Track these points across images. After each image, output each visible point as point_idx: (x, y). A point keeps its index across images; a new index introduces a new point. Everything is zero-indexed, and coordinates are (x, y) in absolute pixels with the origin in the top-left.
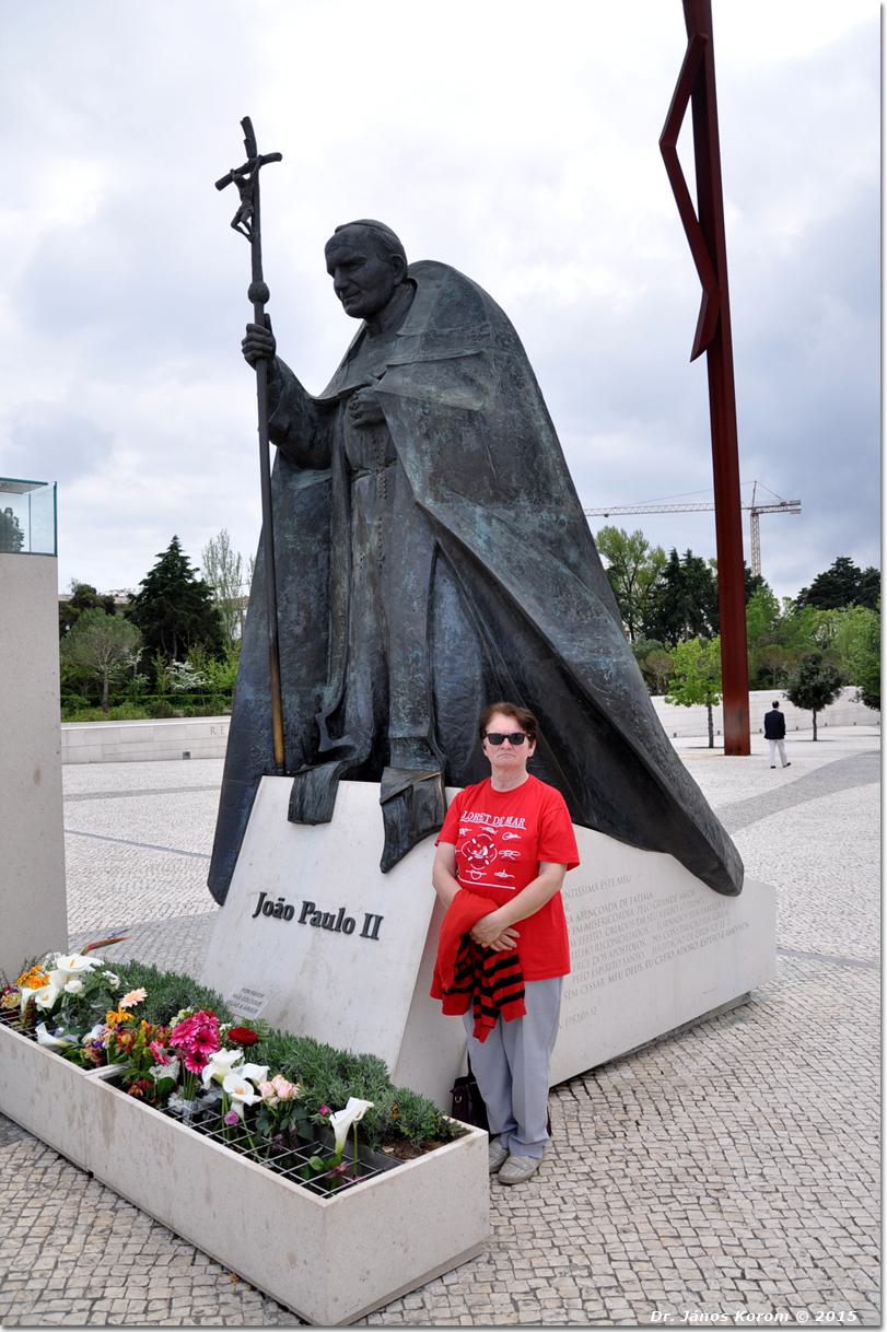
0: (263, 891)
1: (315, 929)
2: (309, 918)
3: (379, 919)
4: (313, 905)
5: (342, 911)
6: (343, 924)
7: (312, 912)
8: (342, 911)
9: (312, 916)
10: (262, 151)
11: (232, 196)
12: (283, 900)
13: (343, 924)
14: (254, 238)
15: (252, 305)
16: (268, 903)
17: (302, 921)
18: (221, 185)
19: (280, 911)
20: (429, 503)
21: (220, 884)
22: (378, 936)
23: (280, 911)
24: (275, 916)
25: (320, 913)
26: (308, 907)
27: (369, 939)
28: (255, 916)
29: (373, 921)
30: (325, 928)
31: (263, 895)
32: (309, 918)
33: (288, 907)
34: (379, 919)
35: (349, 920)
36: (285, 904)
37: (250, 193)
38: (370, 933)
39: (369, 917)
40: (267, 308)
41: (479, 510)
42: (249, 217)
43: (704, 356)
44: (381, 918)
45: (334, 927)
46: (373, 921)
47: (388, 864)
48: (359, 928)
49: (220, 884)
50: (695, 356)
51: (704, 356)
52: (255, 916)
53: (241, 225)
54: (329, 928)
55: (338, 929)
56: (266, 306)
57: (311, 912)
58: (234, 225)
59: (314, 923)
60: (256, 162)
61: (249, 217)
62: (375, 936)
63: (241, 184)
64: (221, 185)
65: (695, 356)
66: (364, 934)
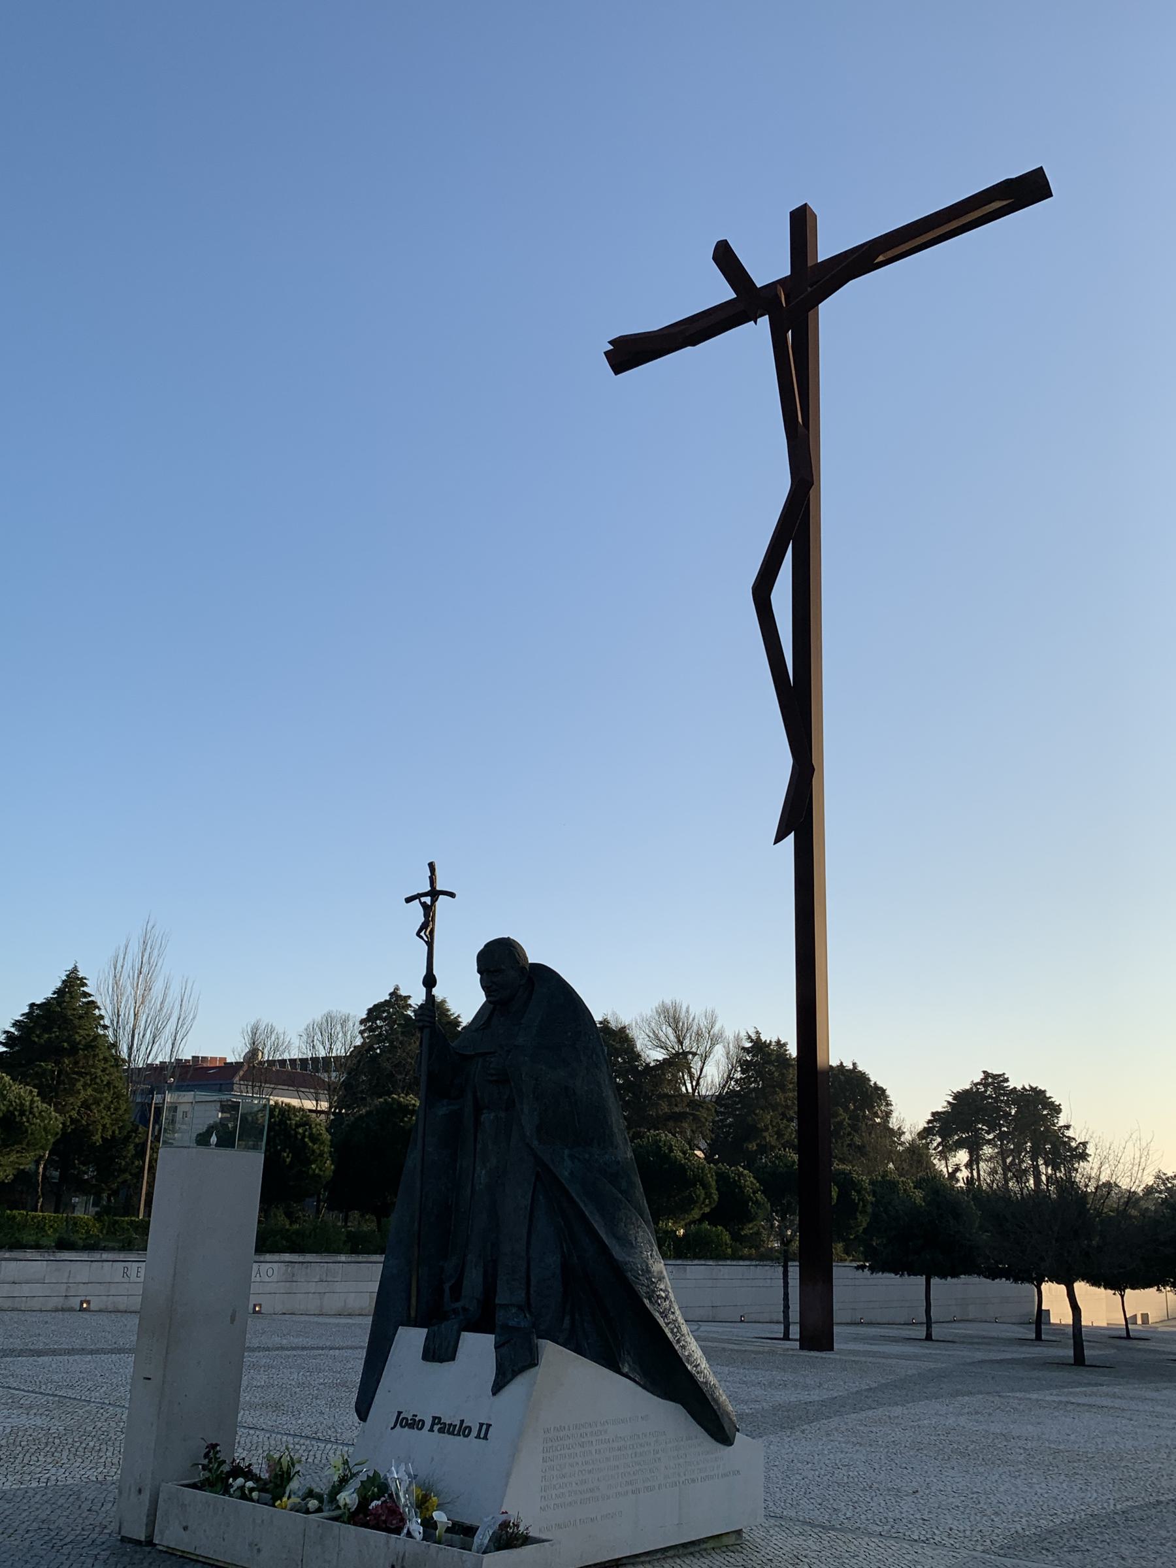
2: (436, 1428)
4: (440, 1419)
5: (462, 1422)
6: (462, 1430)
7: (439, 1423)
8: (462, 1422)
9: (439, 1426)
10: (438, 888)
11: (416, 913)
12: (416, 1416)
13: (462, 1430)
14: (430, 944)
15: (425, 989)
17: (431, 1430)
18: (408, 900)
19: (415, 1424)
20: (535, 1143)
21: (363, 1409)
23: (415, 1424)
25: (445, 1424)
26: (436, 1420)
28: (392, 1429)
29: (484, 1427)
31: (400, 1413)
32: (436, 1428)
33: (420, 1421)
34: (489, 1426)
35: (466, 1427)
36: (417, 1419)
37: (428, 910)
38: (482, 1436)
39: (481, 1425)
40: (435, 991)
41: (566, 1152)
42: (427, 929)
43: (791, 838)
44: (491, 1425)
45: (456, 1433)
46: (484, 1427)
47: (497, 1388)
48: (474, 1433)
49: (363, 1409)
50: (779, 838)
51: (791, 838)
52: (392, 1429)
53: (422, 934)
54: (452, 1434)
56: (433, 989)
58: (418, 934)
59: (441, 1431)
60: (434, 894)
61: (427, 929)
62: (485, 1438)
63: (424, 905)
64: (408, 900)
65: (779, 838)
66: (478, 1437)
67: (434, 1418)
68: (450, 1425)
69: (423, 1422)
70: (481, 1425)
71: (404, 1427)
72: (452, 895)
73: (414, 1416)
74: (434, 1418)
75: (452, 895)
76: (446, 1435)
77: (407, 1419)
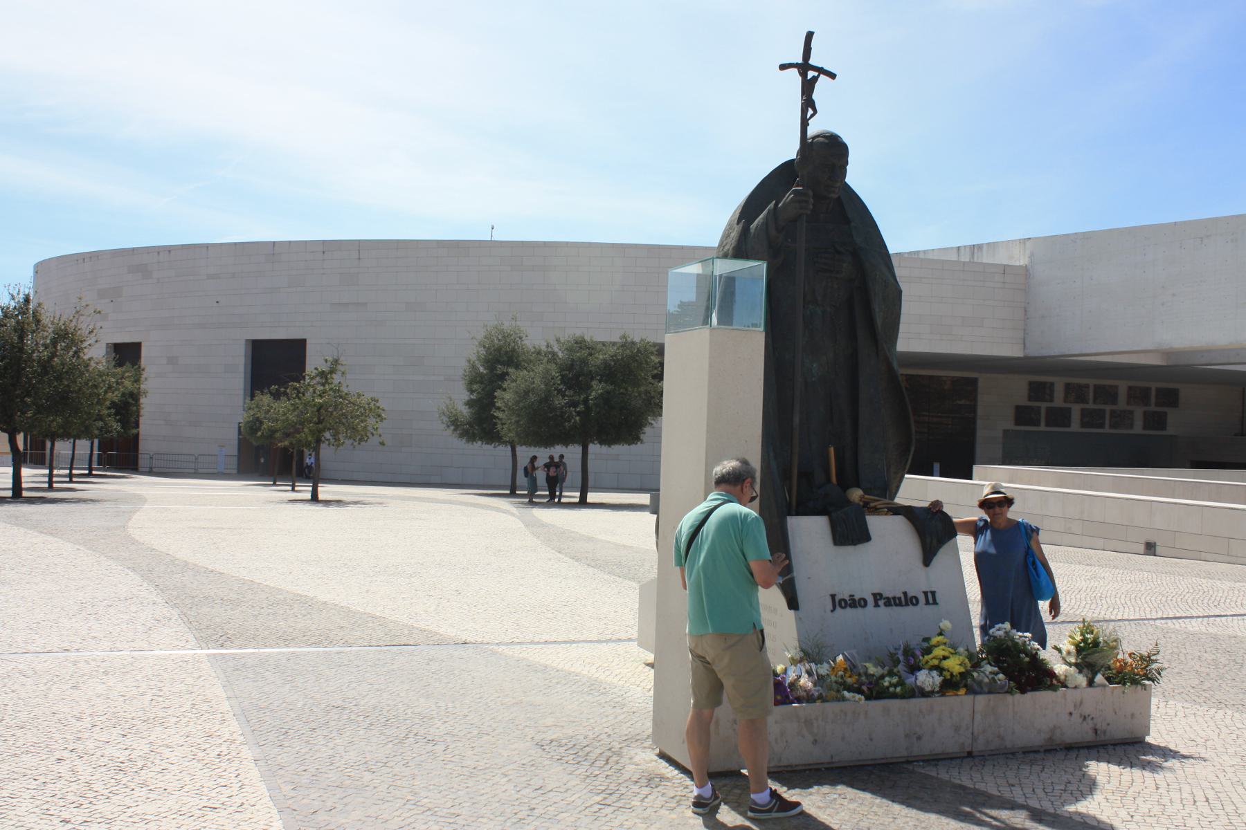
0: (834, 593)
1: (890, 608)
3: (933, 593)
4: (880, 595)
8: (905, 594)
12: (853, 596)
13: (910, 601)
16: (840, 601)
17: (877, 605)
23: (855, 603)
24: (851, 606)
26: (877, 597)
30: (896, 605)
31: (833, 596)
32: (881, 603)
33: (860, 599)
34: (933, 593)
39: (926, 593)
45: (904, 603)
54: (900, 605)
55: (907, 604)
57: (880, 599)
62: (935, 603)
66: (927, 603)
67: (875, 595)
68: (894, 598)
70: (926, 593)
72: (832, 76)
73: (851, 596)
74: (875, 595)
75: (832, 76)
76: (894, 608)
77: (844, 600)
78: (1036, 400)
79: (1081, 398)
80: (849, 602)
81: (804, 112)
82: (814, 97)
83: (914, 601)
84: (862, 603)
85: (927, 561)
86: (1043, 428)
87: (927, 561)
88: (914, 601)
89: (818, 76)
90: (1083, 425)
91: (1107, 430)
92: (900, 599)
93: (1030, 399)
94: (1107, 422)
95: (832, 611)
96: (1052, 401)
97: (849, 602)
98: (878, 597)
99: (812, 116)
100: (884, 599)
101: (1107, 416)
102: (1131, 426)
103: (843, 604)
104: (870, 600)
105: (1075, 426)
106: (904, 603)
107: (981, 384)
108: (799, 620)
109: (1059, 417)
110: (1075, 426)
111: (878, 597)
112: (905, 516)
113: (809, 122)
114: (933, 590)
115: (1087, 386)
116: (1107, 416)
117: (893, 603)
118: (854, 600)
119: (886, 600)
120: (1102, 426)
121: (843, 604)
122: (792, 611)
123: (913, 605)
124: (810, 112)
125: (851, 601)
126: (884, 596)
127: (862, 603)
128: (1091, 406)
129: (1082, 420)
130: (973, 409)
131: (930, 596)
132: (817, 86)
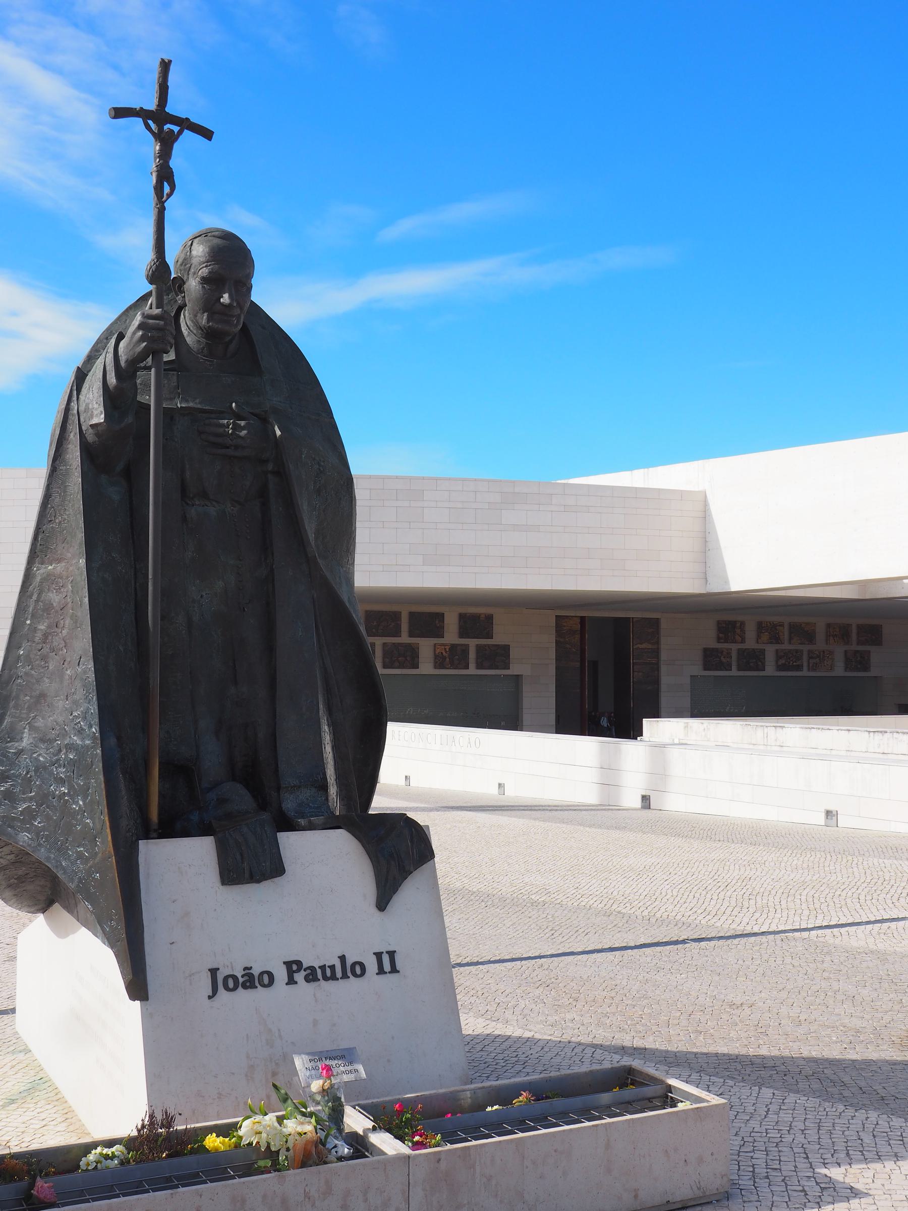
3: (392, 954)
4: (299, 963)
5: (343, 958)
6: (357, 970)
8: (343, 958)
9: (303, 974)
16: (226, 979)
17: (291, 981)
22: (399, 966)
24: (245, 987)
25: (312, 968)
26: (293, 967)
27: (388, 974)
30: (325, 978)
31: (214, 972)
32: (300, 977)
33: (262, 973)
34: (392, 954)
35: (354, 964)
39: (379, 955)
45: (339, 974)
48: (371, 965)
54: (333, 977)
55: (345, 976)
57: (298, 970)
59: (312, 976)
62: (394, 970)
66: (381, 971)
67: (288, 964)
68: (323, 968)
69: (271, 975)
71: (235, 988)
72: (207, 134)
73: (245, 969)
74: (288, 964)
75: (207, 134)
76: (322, 982)
77: (234, 977)
78: (726, 642)
79: (776, 639)
80: (241, 980)
81: (159, 189)
82: (172, 164)
83: (358, 970)
84: (266, 979)
85: (382, 904)
86: (734, 672)
87: (382, 904)
88: (358, 970)
89: (180, 132)
90: (780, 668)
91: (805, 673)
92: (332, 967)
93: (719, 640)
94: (805, 664)
95: (210, 997)
96: (743, 641)
97: (241, 980)
98: (295, 967)
99: (169, 195)
100: (305, 970)
101: (805, 657)
102: (832, 668)
103: (231, 984)
104: (281, 974)
105: (770, 670)
106: (339, 974)
107: (663, 625)
108: (146, 1017)
109: (752, 660)
110: (770, 670)
111: (295, 967)
112: (345, 829)
113: (166, 204)
114: (391, 949)
115: (782, 625)
116: (805, 657)
117: (320, 975)
118: (251, 976)
119: (309, 971)
120: (799, 668)
121: (231, 984)
122: (138, 1003)
123: (355, 975)
124: (167, 189)
125: (246, 978)
126: (305, 966)
127: (267, 979)
128: (786, 646)
129: (777, 662)
130: (656, 653)
131: (386, 959)
132: (178, 148)
